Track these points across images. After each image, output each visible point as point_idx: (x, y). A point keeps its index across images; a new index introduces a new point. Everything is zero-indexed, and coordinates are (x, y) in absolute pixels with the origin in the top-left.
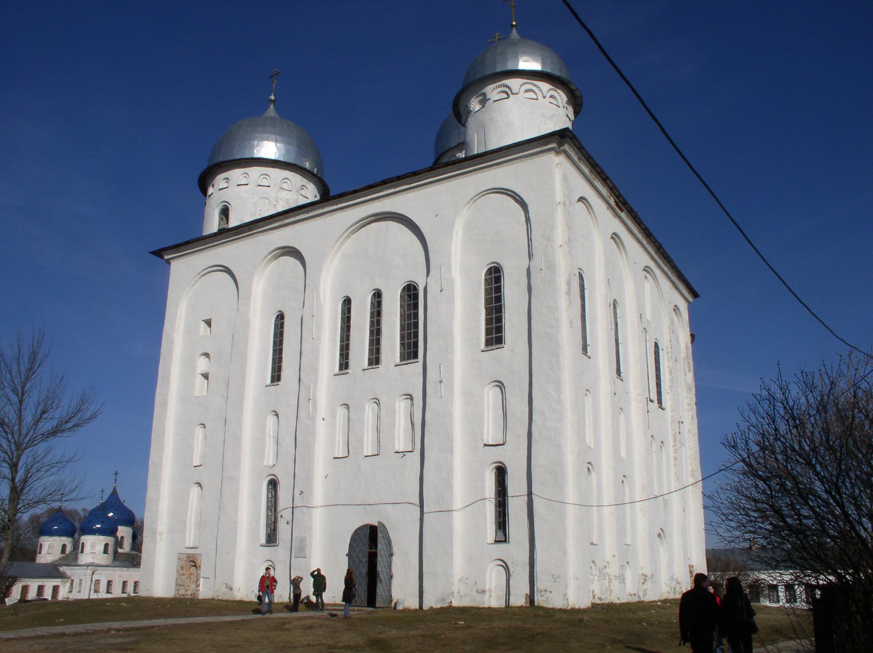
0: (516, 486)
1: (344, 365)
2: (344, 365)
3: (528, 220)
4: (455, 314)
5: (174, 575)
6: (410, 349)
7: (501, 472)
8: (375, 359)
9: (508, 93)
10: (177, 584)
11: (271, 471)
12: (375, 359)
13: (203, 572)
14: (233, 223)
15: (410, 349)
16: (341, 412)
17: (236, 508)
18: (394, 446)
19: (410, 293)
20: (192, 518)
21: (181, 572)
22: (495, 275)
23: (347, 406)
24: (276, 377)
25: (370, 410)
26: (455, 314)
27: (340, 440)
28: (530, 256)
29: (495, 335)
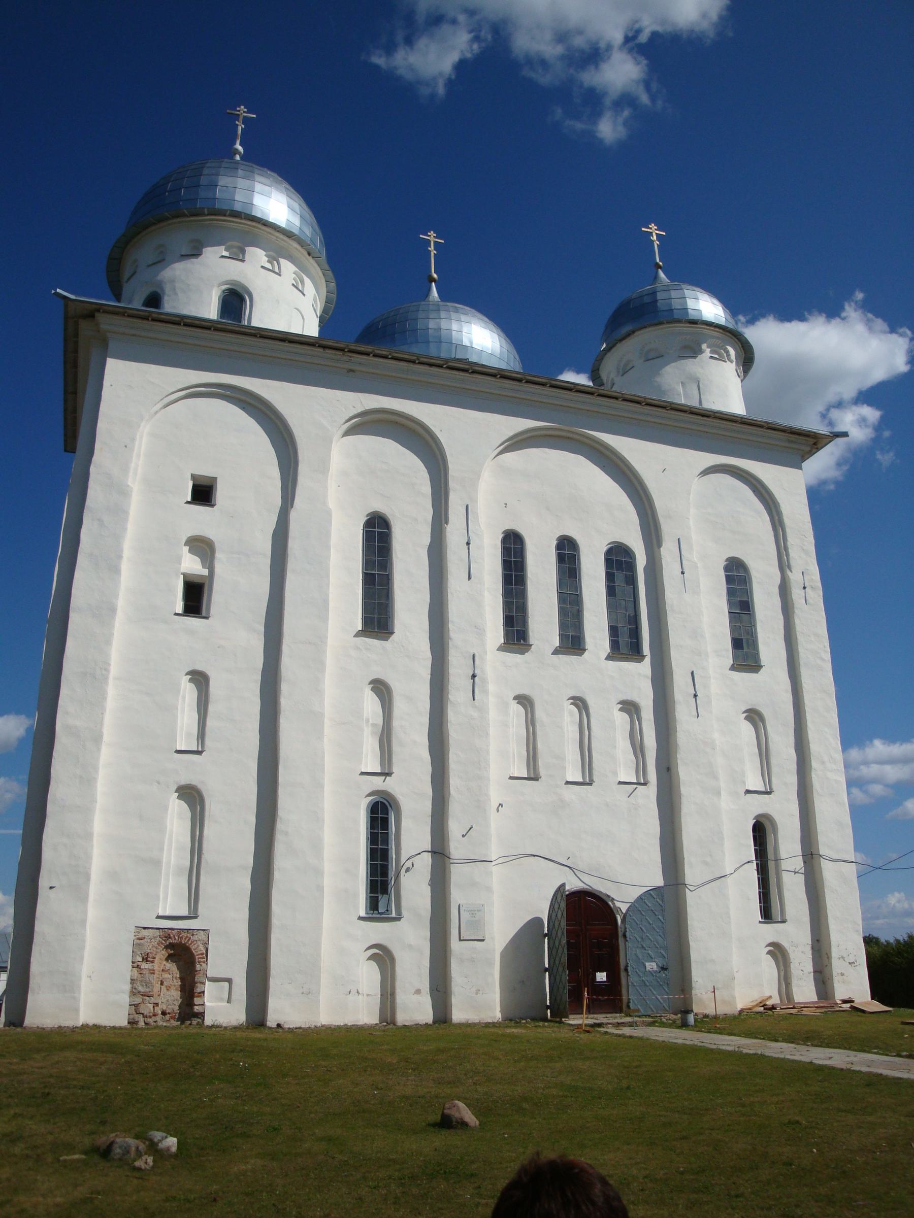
5: (126, 971)
8: (572, 641)
10: (133, 993)
12: (572, 641)
13: (214, 966)
15: (625, 644)
16: (517, 710)
18: (615, 773)
21: (144, 965)
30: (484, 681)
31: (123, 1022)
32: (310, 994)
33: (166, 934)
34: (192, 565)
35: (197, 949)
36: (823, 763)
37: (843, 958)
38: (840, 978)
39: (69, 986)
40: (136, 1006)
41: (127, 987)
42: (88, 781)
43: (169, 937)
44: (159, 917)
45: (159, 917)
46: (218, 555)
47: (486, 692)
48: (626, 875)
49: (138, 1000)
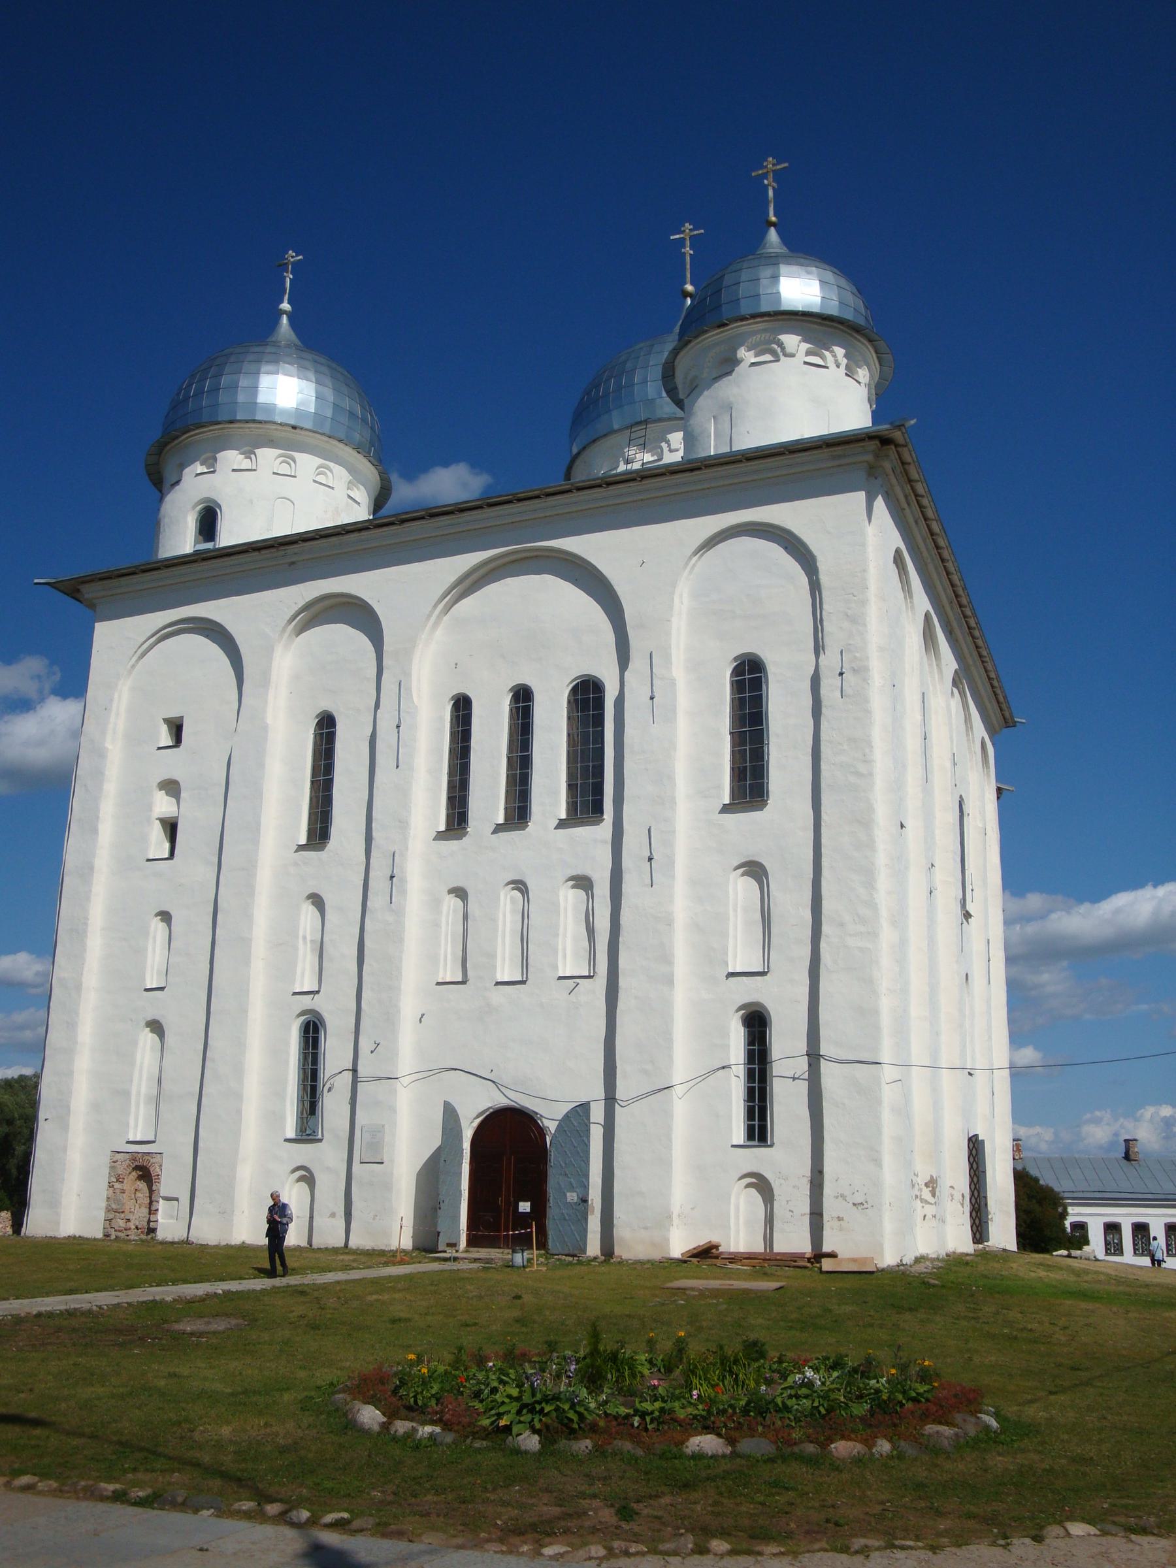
0: (787, 1046)
1: (458, 818)
2: (458, 818)
3: (815, 587)
4: (676, 742)
5: (103, 1191)
6: (587, 799)
7: (757, 1023)
8: (518, 812)
9: (777, 353)
10: (109, 1210)
11: (307, 1002)
12: (518, 812)
13: (165, 1187)
14: (229, 535)
15: (587, 799)
17: (239, 1070)
18: (555, 967)
19: (587, 697)
20: (142, 1086)
21: (117, 1185)
22: (749, 677)
23: (460, 893)
24: (320, 830)
25: (508, 902)
26: (676, 742)
27: (449, 951)
28: (818, 648)
29: (749, 783)
30: (403, 881)
31: (100, 1235)
32: (226, 1213)
33: (133, 1156)
34: (164, 805)
35: (154, 1170)
36: (842, 925)
37: (842, 1196)
38: (836, 1224)
39: (54, 1204)
40: (110, 1220)
41: (104, 1204)
42: (72, 1026)
43: (135, 1160)
44: (128, 1142)
45: (128, 1142)
46: (183, 795)
47: (404, 893)
48: (552, 1088)
49: (111, 1216)
